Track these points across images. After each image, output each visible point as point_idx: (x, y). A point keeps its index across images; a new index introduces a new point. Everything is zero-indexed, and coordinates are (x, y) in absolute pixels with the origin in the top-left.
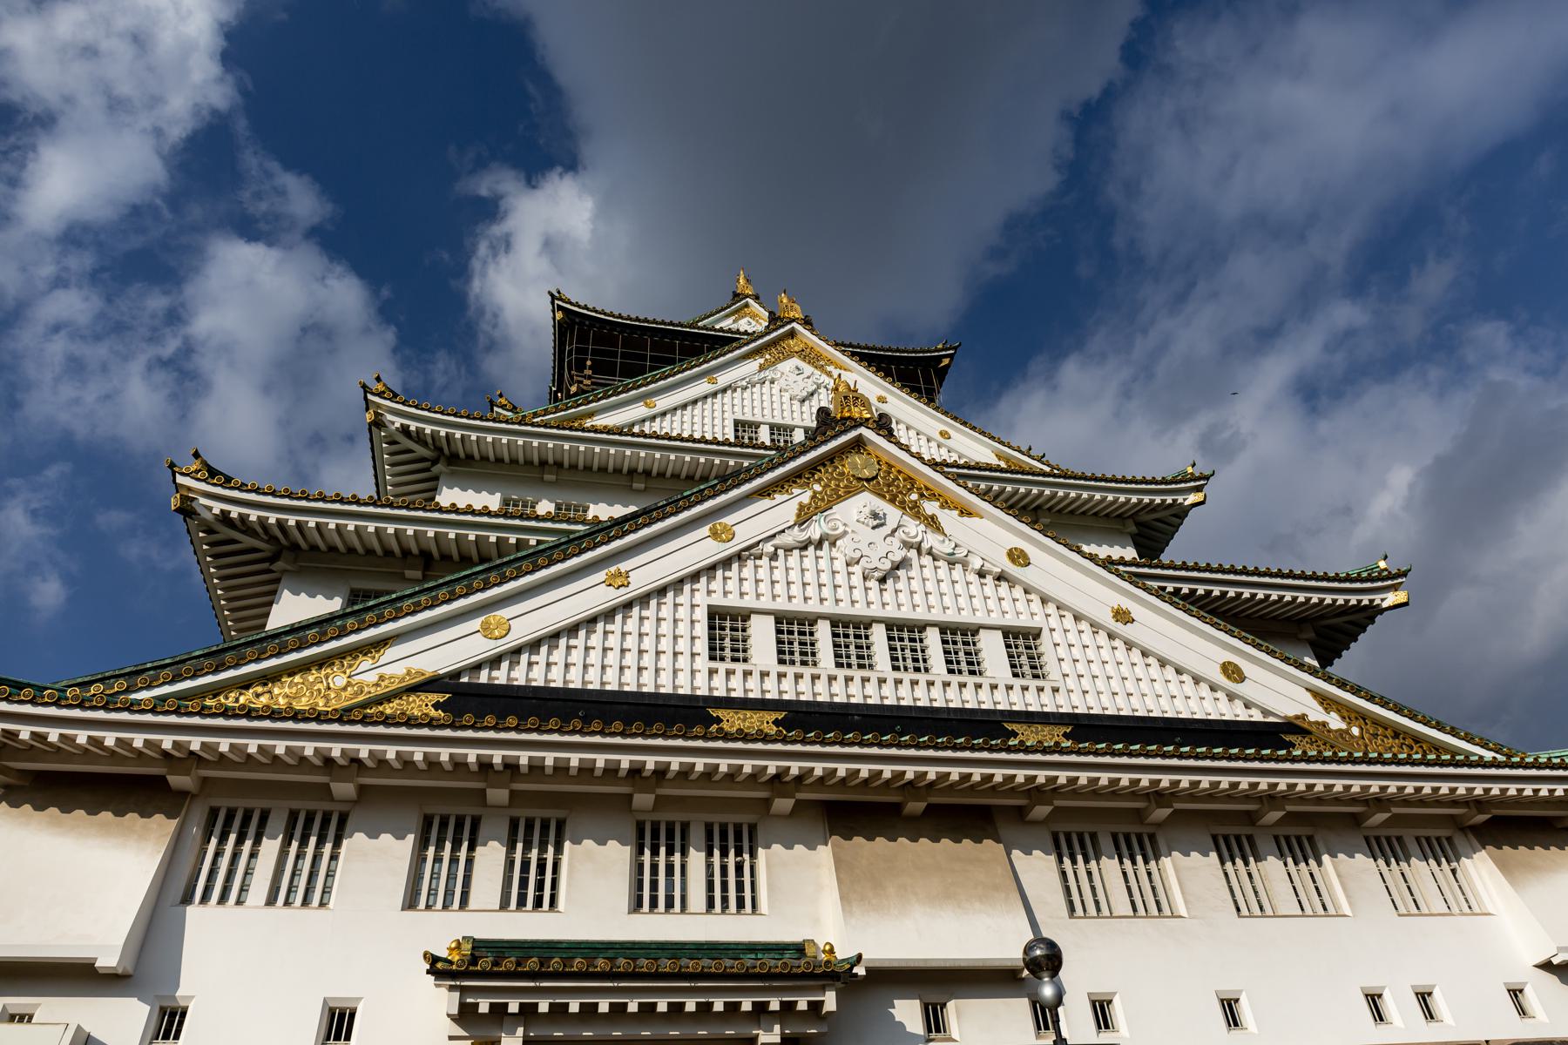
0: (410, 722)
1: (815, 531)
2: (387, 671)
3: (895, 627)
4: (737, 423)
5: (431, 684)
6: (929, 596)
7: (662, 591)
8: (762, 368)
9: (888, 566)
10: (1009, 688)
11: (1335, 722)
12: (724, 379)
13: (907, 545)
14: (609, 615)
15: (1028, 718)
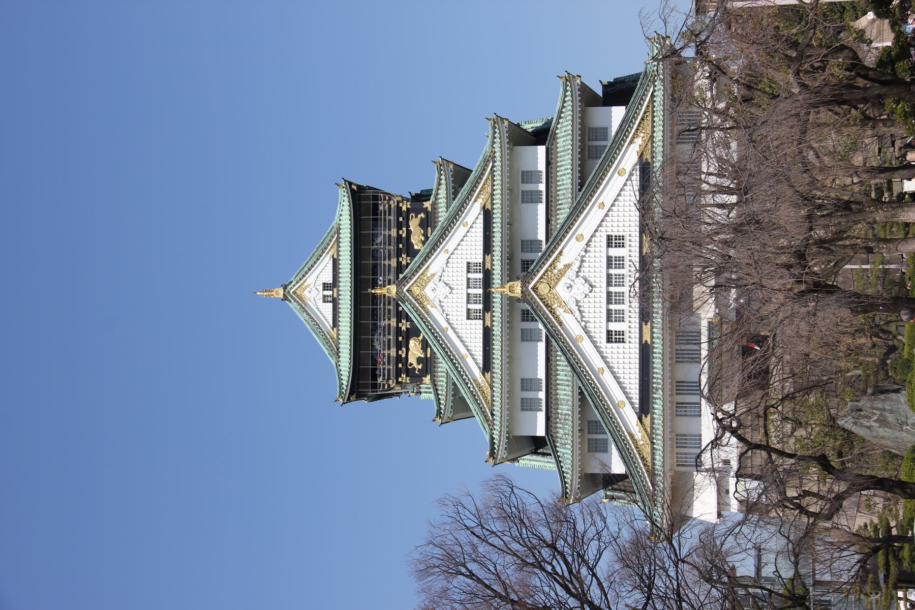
0: (652, 423)
1: (575, 308)
2: (637, 430)
3: (609, 284)
4: (468, 318)
5: (640, 419)
6: (597, 270)
7: (603, 357)
8: (434, 306)
9: (587, 285)
10: (630, 251)
11: (639, 141)
12: (444, 324)
13: (577, 276)
14: (613, 373)
15: (641, 247)
